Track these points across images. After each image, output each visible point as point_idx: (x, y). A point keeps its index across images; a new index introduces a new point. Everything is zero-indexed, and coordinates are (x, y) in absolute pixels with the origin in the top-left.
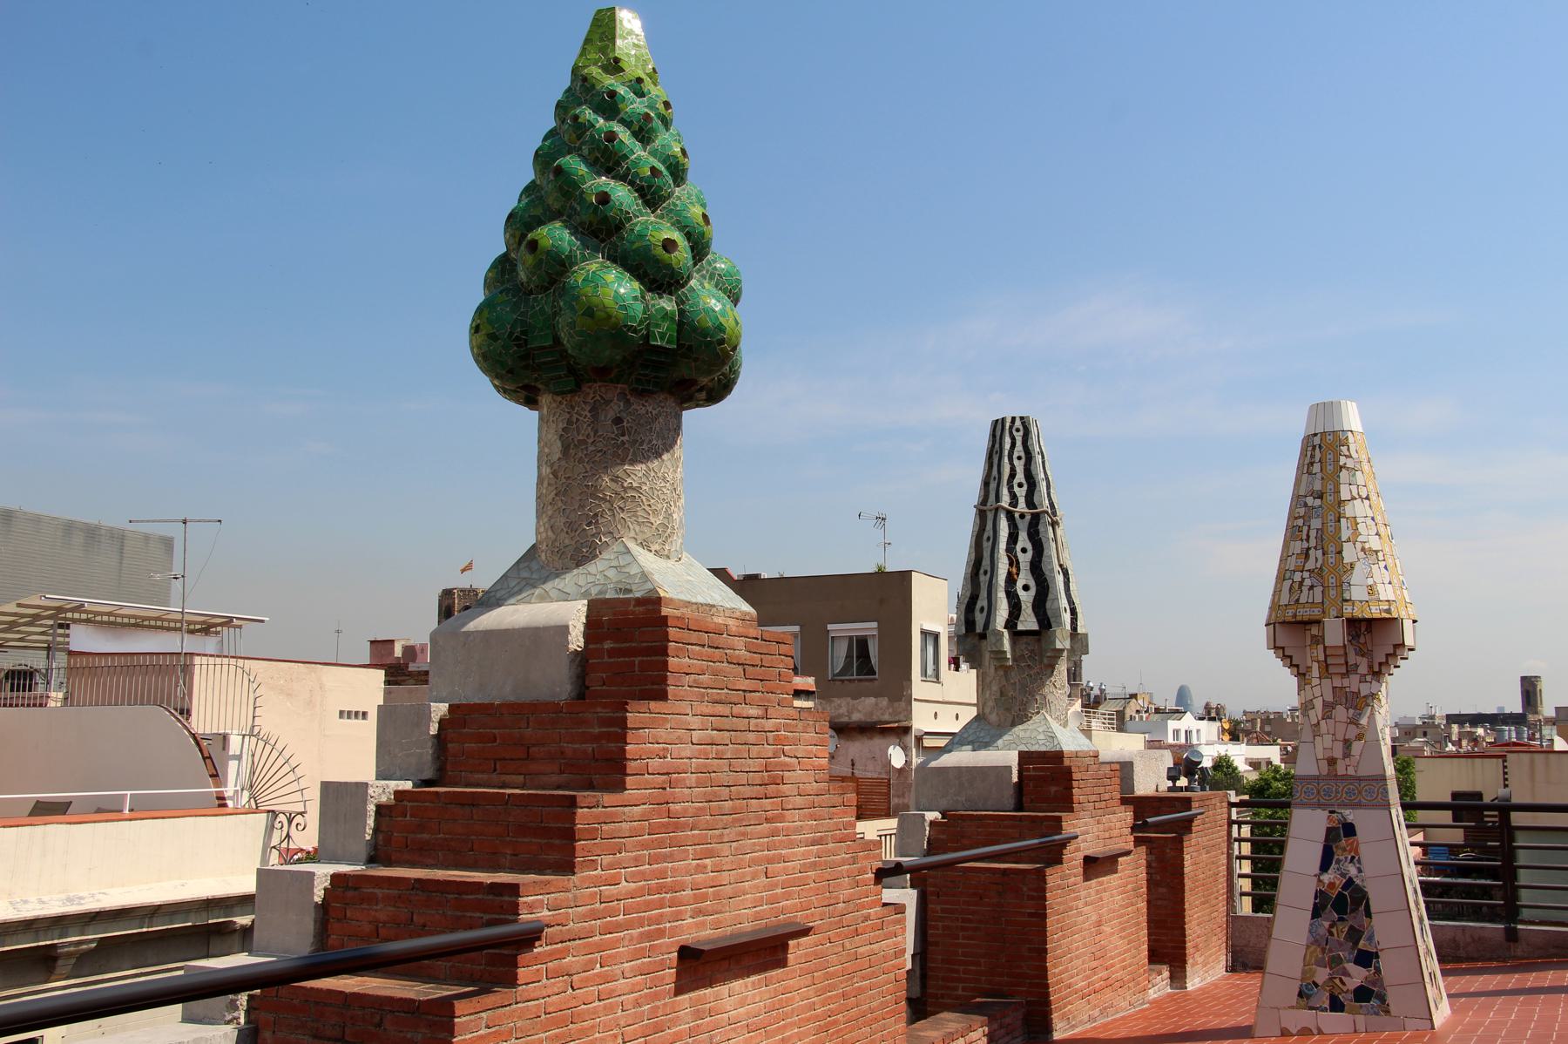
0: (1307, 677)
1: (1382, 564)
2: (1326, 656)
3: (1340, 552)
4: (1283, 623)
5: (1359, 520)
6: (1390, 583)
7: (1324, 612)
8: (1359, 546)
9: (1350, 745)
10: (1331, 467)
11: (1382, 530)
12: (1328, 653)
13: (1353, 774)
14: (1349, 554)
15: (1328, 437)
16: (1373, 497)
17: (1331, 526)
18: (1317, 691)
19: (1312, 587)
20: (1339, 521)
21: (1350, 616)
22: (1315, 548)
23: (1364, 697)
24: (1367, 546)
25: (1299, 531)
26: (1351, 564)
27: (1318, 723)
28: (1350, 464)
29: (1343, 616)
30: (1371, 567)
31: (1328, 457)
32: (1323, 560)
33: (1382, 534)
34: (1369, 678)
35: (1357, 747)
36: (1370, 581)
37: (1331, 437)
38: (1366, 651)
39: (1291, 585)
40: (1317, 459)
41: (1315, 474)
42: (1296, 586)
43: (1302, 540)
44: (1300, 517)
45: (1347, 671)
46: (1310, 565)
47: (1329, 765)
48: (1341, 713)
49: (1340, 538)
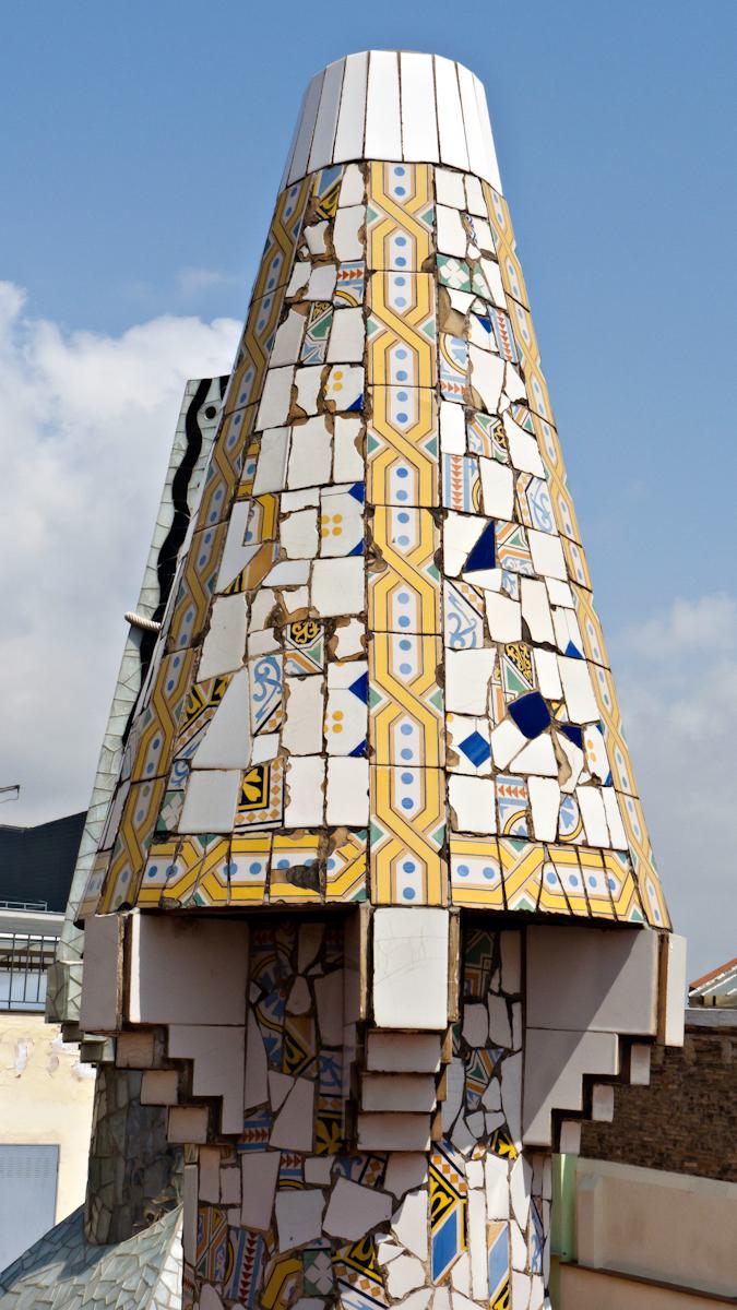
1: (343, 676)
3: (198, 641)
6: (363, 750)
8: (264, 604)
16: (393, 406)
21: (149, 898)
23: (297, 1253)
24: (293, 602)
30: (286, 692)
34: (318, 1170)
36: (264, 749)
38: (311, 1051)
49: (212, 584)
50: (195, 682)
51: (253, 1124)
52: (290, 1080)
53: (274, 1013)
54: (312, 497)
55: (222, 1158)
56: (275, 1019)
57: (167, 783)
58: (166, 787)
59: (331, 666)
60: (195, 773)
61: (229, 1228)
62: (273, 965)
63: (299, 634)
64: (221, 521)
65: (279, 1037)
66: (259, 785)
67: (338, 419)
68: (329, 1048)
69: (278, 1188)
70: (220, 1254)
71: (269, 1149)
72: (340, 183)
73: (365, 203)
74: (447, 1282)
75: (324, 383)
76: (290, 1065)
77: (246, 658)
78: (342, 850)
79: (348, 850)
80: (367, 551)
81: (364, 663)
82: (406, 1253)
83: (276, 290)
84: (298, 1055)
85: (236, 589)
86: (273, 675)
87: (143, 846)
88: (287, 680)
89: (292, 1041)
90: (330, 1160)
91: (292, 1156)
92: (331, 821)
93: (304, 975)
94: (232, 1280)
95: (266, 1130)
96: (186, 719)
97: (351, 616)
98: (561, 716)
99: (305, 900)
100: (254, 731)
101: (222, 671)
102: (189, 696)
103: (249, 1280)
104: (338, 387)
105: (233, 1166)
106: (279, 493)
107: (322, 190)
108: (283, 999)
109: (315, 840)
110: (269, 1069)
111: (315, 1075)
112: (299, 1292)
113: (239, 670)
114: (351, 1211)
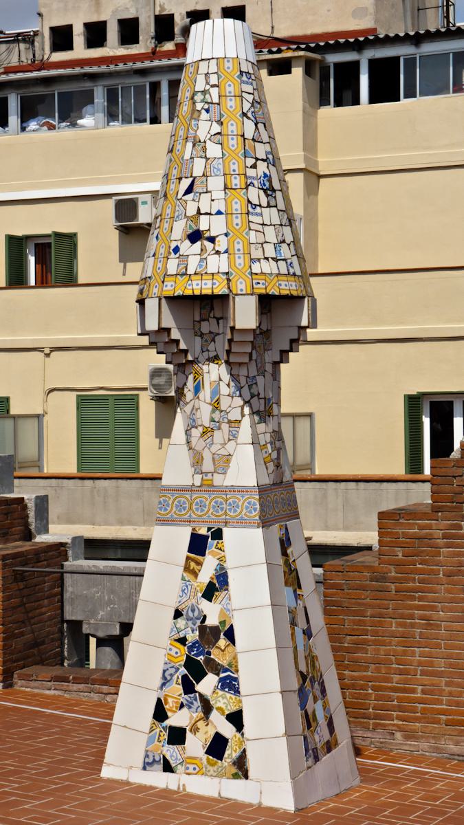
74: (198, 398)
98: (207, 235)
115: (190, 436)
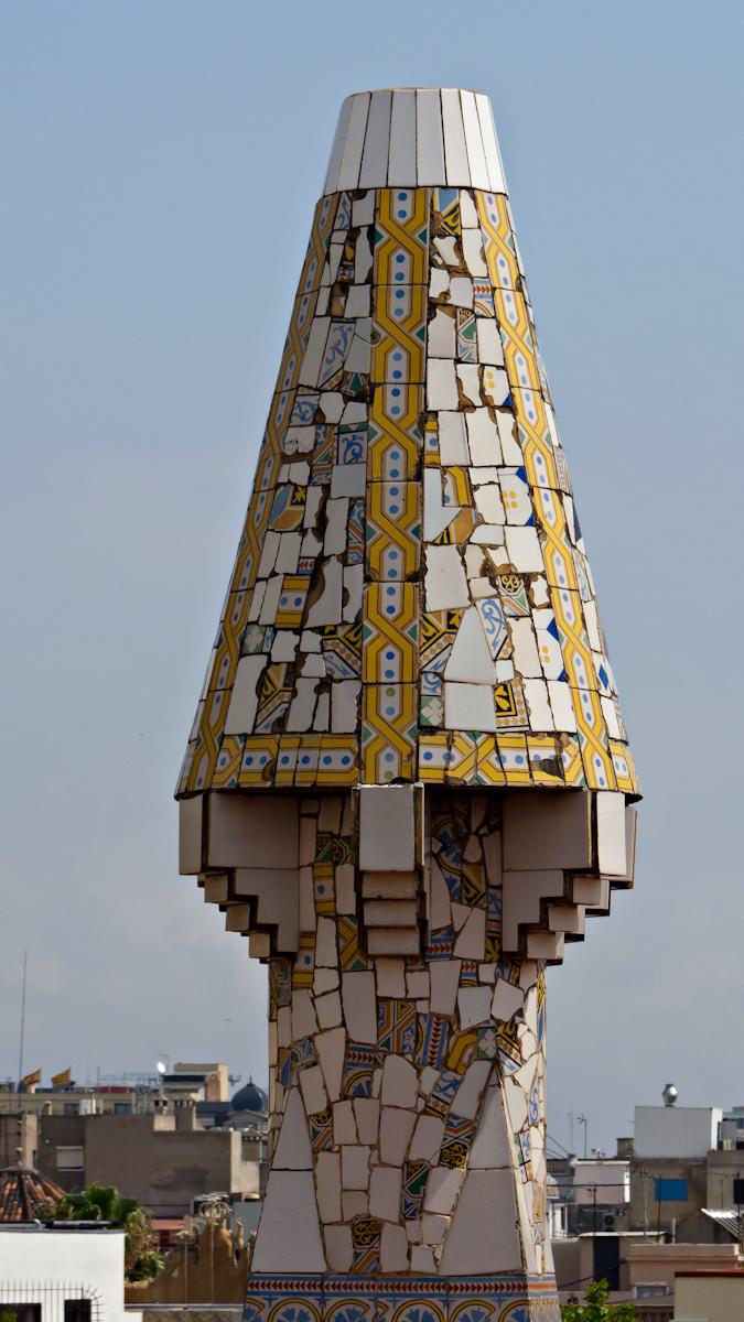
0: (300, 965)
1: (542, 618)
2: (361, 902)
3: (417, 576)
4: (236, 793)
5: (477, 477)
6: (564, 678)
7: (360, 763)
8: (475, 557)
9: (424, 1180)
10: (404, 303)
11: (548, 507)
12: (367, 892)
13: (429, 1267)
14: (445, 583)
15: (398, 206)
16: (527, 403)
17: (394, 491)
18: (329, 1011)
19: (325, 685)
20: (419, 477)
21: (436, 777)
22: (344, 559)
23: (473, 1031)
24: (498, 558)
25: (295, 503)
26: (450, 616)
27: (329, 1109)
28: (461, 294)
29: (417, 780)
30: (509, 630)
31: (396, 268)
32: (365, 598)
33: (549, 523)
34: (487, 972)
35: (444, 1188)
36: (504, 672)
37: (407, 206)
38: (482, 888)
39: (264, 672)
40: (360, 274)
41: (354, 320)
42: (278, 677)
43: (302, 531)
44: (299, 457)
45: (423, 948)
46: (325, 611)
47: (358, 1241)
48: (398, 1078)
49: (418, 531)
50: (424, 610)
51: (438, 941)
52: (468, 909)
53: (453, 861)
54: (491, 475)
55: (406, 965)
56: (454, 865)
57: (419, 690)
58: (419, 692)
59: (533, 610)
60: (448, 685)
61: (418, 1015)
62: (450, 825)
63: (507, 584)
64: (408, 480)
65: (459, 879)
66: (507, 698)
67: (497, 412)
68: (494, 887)
69: (460, 985)
70: (409, 1033)
71: (452, 958)
72: (458, 206)
73: (479, 227)
75: (481, 380)
76: (466, 898)
77: (470, 598)
78: (567, 748)
79: (569, 748)
80: (534, 522)
81: (550, 610)
82: (529, 1030)
83: (412, 284)
84: (473, 891)
85: (446, 541)
86: (496, 615)
87: (406, 735)
88: (508, 620)
89: (469, 882)
90: (495, 965)
91: (469, 963)
92: (558, 729)
93: (476, 833)
94: (422, 1050)
95: (449, 944)
96: (424, 640)
97: (537, 574)
99: (555, 784)
100: (494, 655)
101: (455, 606)
102: (420, 622)
103: (437, 1050)
104: (493, 386)
105: (421, 971)
106: (466, 468)
107: (442, 207)
108: (460, 851)
109: (551, 741)
110: (452, 900)
111: (485, 906)
112: (475, 1056)
113: (468, 608)
114: (503, 1002)
115: (528, 1146)
